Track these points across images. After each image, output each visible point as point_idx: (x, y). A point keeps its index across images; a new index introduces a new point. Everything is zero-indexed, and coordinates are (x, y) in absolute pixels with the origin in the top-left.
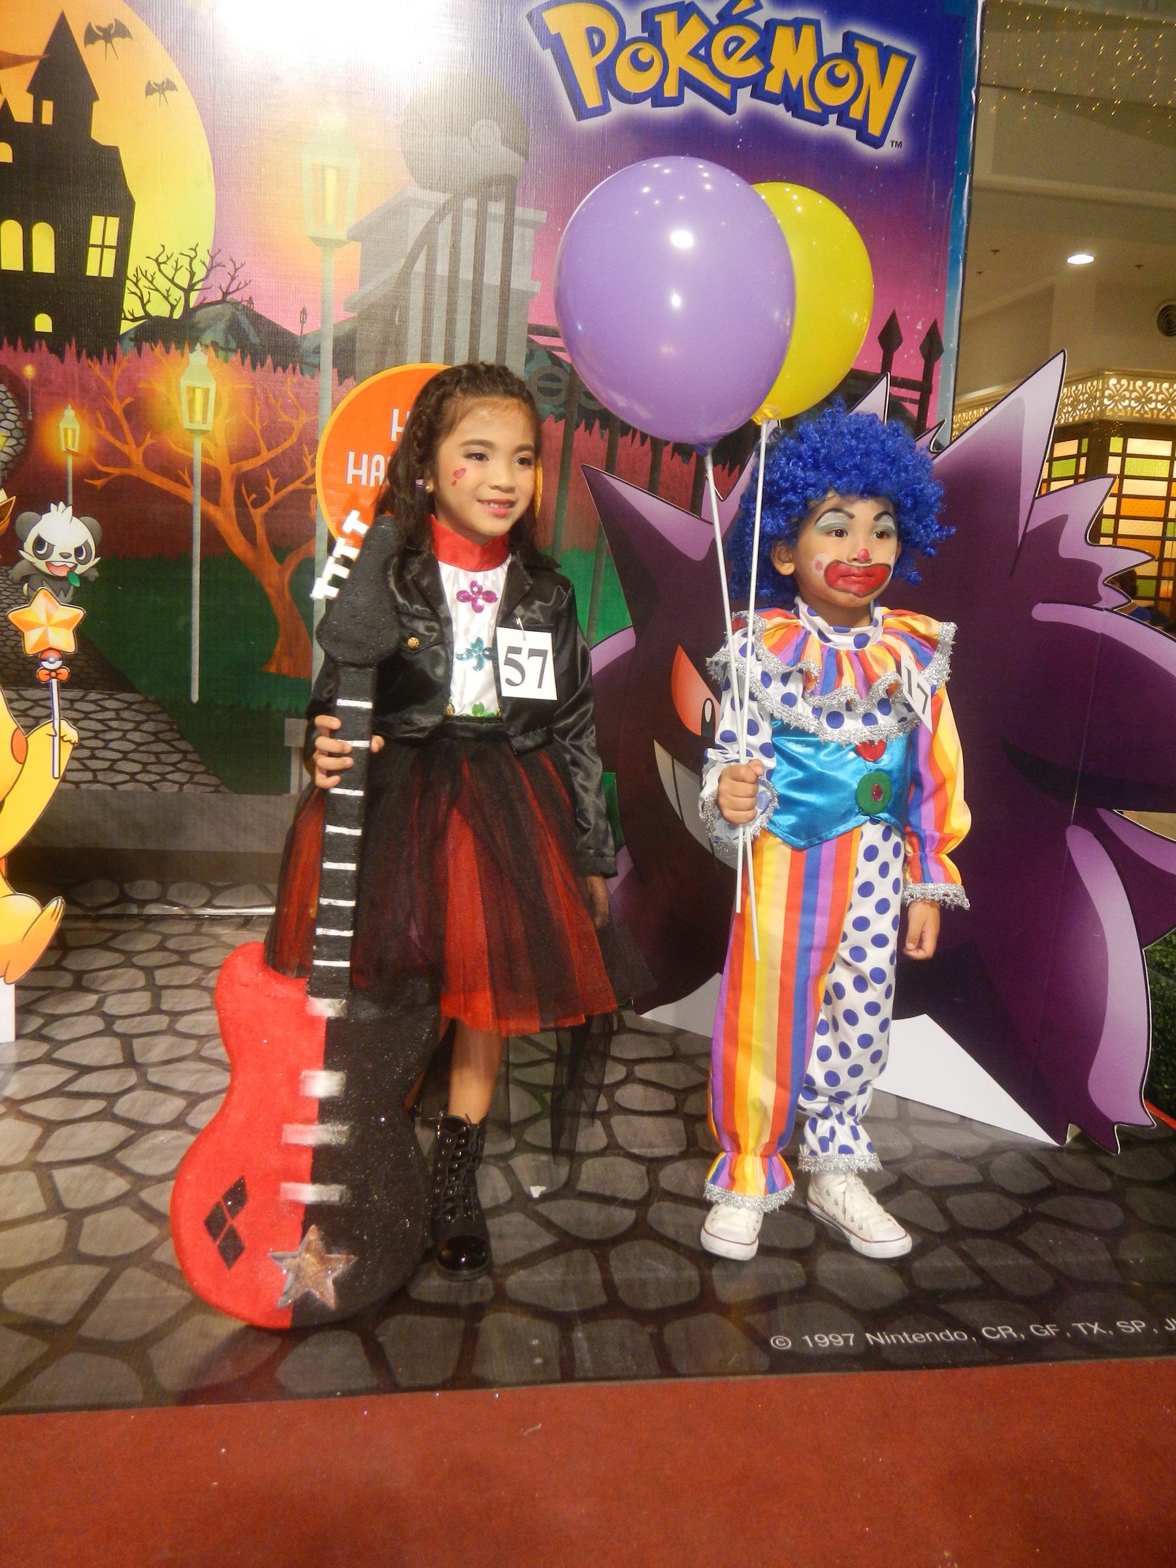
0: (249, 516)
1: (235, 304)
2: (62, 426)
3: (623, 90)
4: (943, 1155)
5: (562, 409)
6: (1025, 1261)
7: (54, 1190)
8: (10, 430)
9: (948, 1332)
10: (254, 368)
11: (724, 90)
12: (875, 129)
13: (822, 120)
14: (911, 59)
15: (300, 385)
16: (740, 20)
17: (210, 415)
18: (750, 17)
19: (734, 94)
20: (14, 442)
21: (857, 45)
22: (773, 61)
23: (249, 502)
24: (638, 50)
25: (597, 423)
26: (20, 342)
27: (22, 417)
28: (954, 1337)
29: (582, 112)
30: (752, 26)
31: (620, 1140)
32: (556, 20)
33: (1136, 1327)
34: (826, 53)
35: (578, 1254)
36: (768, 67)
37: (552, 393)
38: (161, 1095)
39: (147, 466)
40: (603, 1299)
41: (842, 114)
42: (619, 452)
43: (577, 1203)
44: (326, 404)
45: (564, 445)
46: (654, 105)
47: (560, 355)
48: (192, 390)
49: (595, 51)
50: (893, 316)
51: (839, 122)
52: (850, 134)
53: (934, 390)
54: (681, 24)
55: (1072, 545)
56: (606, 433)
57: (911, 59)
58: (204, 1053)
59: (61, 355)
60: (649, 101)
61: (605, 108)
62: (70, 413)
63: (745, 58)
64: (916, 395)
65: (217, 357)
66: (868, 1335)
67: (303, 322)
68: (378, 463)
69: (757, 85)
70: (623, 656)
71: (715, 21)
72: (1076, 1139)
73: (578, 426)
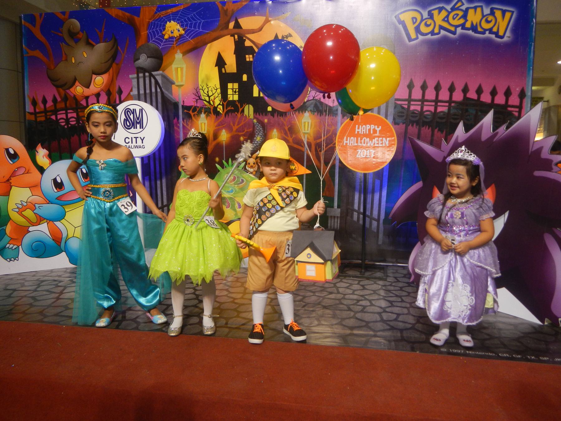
0: (318, 154)
1: (316, 100)
2: (273, 134)
3: (422, 33)
4: (504, 323)
5: (405, 121)
6: (518, 344)
7: (275, 309)
8: (261, 136)
9: (490, 353)
10: (321, 116)
11: (453, 29)
12: (501, 33)
13: (484, 33)
14: (513, 12)
15: (332, 119)
16: (458, 9)
17: (309, 129)
18: (461, 8)
19: (456, 30)
20: (262, 138)
21: (495, 11)
22: (468, 18)
23: (318, 150)
24: (426, 22)
25: (415, 124)
26: (264, 114)
27: (264, 132)
28: (490, 354)
29: (410, 39)
30: (462, 10)
31: (411, 313)
32: (402, 17)
33: (545, 359)
34: (485, 14)
35: (395, 331)
36: (467, 21)
37: (402, 116)
38: (297, 296)
39: (293, 143)
40: (400, 338)
41: (491, 31)
42: (421, 132)
43: (397, 323)
44: (339, 124)
45: (405, 131)
46: (432, 35)
47: (404, 106)
48: (305, 123)
49: (414, 23)
50: (509, 87)
51: (490, 33)
52: (493, 36)
53: (523, 108)
54: (439, 13)
55: (546, 154)
56: (418, 128)
57: (513, 12)
58: (306, 289)
59: (273, 116)
60: (430, 35)
61: (417, 38)
62: (275, 130)
63: (459, 19)
64: (517, 110)
65: (311, 113)
66: (467, 352)
67: (333, 103)
68: (352, 139)
69: (463, 26)
70: (420, 188)
71: (450, 10)
72: (549, 324)
73: (409, 125)
